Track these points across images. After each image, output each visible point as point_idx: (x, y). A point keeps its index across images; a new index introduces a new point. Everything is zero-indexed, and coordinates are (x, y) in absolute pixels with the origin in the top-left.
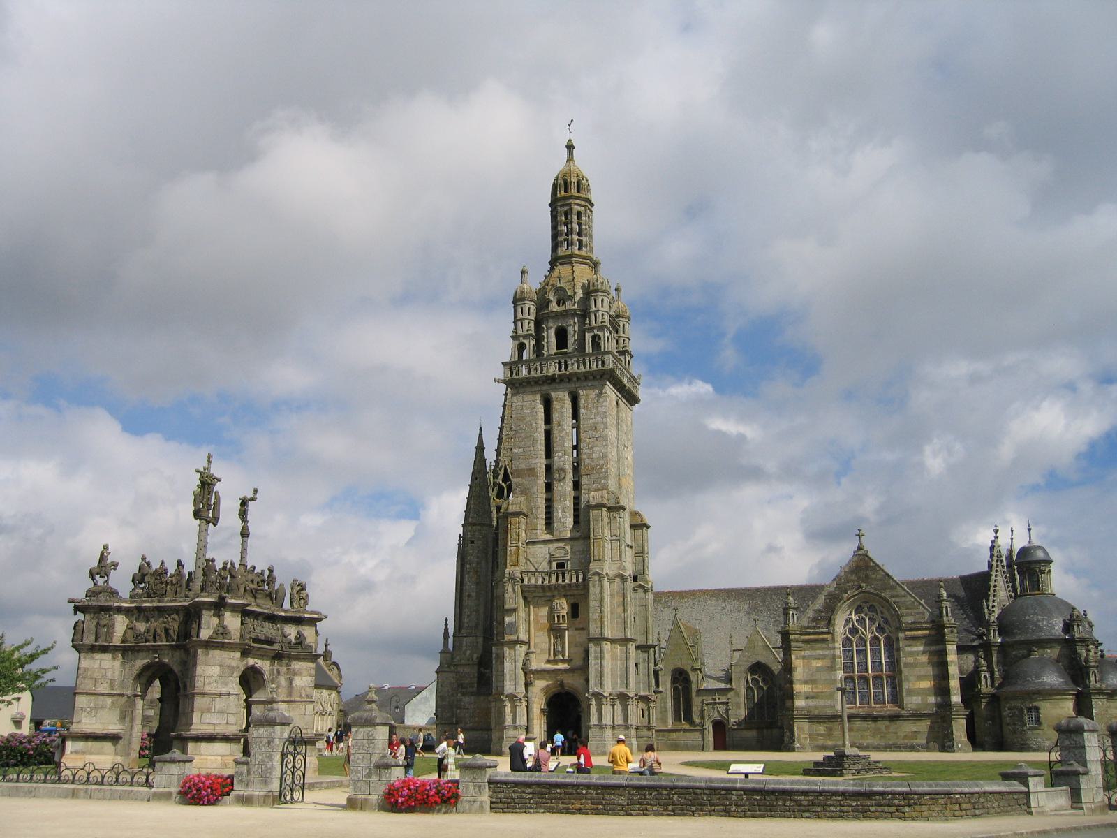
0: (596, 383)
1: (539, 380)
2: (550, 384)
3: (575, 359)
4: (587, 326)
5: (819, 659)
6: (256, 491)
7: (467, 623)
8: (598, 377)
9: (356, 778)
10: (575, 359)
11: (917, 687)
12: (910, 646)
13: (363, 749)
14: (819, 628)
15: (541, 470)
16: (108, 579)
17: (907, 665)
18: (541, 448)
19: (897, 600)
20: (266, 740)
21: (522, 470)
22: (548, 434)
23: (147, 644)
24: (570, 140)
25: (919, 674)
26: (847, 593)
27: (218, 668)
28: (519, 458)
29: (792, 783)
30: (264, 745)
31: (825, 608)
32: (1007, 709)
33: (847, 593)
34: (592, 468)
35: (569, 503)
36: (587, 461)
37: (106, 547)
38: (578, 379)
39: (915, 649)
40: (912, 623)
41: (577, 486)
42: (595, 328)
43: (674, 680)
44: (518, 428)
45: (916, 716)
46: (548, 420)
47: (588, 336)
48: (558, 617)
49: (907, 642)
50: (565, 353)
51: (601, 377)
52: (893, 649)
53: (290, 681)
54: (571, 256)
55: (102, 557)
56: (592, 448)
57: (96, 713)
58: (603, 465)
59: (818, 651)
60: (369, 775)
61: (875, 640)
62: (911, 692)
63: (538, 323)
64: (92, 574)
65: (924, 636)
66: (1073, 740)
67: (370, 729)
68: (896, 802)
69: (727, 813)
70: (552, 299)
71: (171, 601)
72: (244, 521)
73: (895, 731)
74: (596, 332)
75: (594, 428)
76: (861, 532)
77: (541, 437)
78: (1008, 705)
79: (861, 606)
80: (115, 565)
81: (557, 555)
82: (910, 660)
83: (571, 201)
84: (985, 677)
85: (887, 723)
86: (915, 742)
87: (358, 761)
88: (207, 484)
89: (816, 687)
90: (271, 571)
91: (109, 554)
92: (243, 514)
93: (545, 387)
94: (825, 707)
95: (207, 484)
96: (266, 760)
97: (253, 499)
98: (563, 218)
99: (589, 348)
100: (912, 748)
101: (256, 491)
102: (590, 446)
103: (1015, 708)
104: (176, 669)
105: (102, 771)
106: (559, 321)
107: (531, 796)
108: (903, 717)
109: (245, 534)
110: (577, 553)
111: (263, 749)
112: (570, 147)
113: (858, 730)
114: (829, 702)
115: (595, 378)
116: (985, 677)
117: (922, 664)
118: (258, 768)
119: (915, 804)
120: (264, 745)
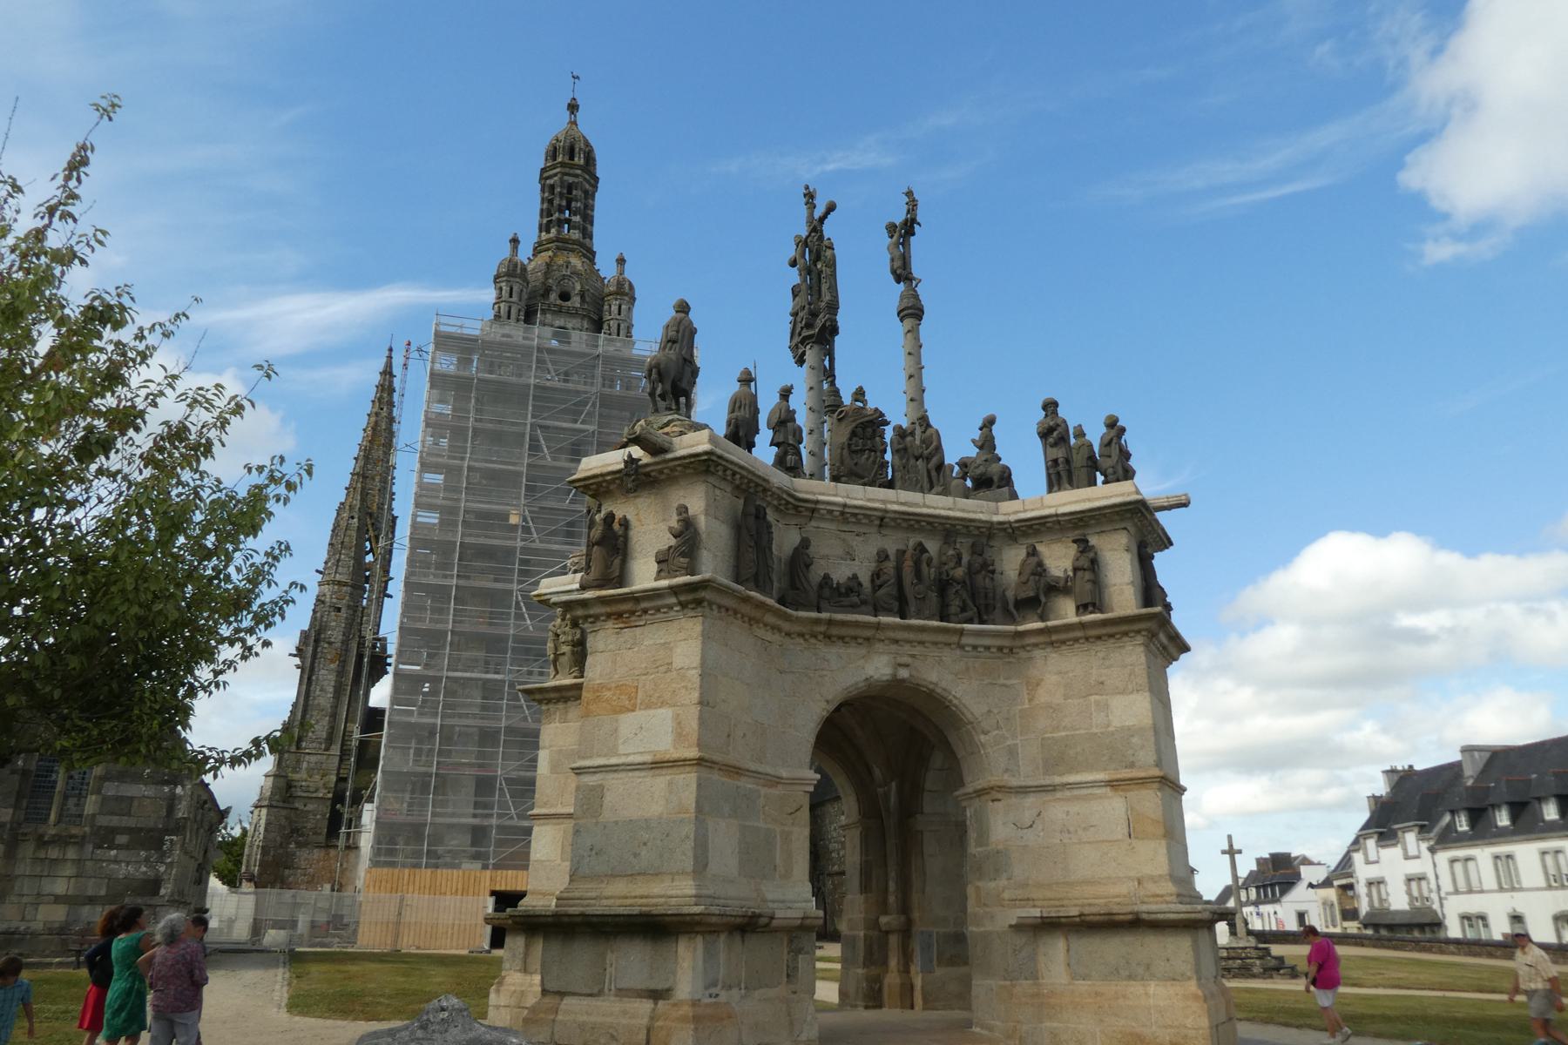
37: (683, 308)
70: (554, 288)
83: (579, 172)
98: (565, 191)
106: (562, 320)
112: (573, 107)
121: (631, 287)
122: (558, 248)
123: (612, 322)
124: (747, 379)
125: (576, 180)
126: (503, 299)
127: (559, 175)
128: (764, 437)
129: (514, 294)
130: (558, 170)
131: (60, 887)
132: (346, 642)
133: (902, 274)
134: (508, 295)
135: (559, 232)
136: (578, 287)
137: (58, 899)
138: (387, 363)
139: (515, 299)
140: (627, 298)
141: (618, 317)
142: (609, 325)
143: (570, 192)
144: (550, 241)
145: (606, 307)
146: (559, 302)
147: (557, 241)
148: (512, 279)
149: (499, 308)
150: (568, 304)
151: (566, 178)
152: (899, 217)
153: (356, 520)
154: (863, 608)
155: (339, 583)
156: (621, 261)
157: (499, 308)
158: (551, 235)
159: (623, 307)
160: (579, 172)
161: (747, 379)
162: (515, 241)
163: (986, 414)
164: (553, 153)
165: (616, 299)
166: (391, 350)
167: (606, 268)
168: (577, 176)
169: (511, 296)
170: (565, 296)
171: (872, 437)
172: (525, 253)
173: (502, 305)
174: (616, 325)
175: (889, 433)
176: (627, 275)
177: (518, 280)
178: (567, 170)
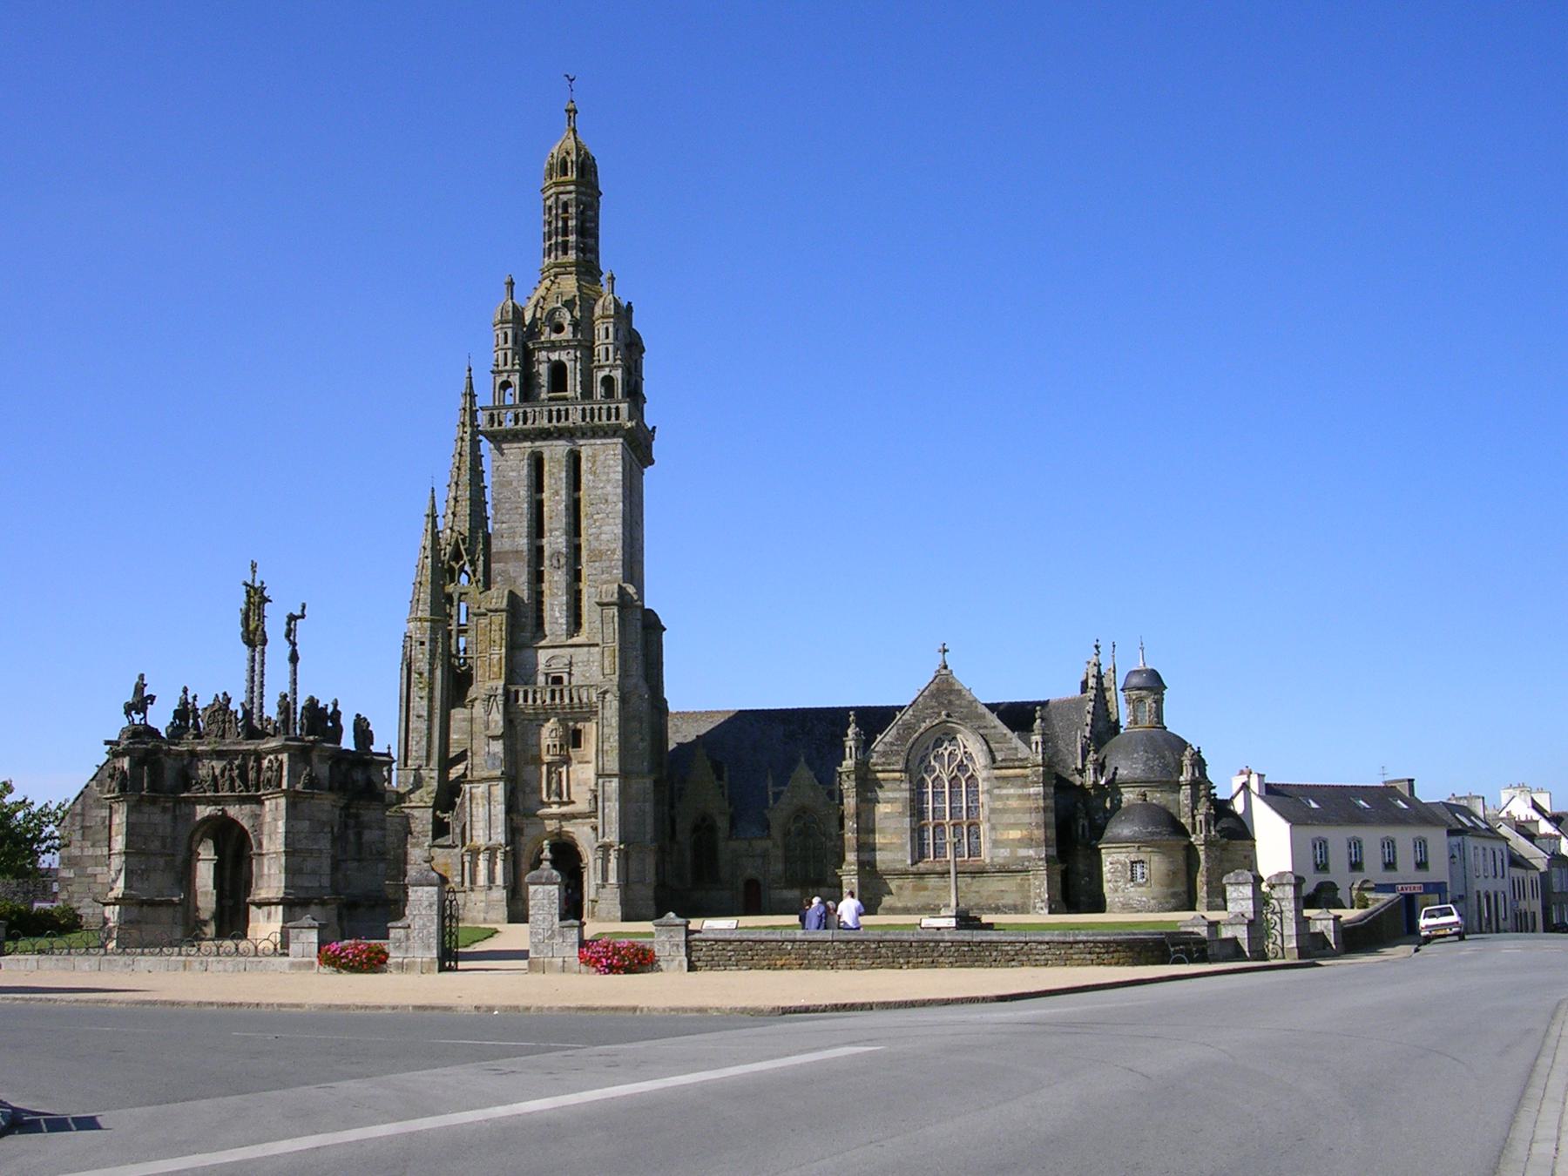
1: (530, 433)
4: (596, 363)
5: (888, 802)
6: (304, 607)
7: (416, 751)
8: (610, 433)
9: (537, 940)
11: (1005, 837)
12: (998, 788)
13: (543, 910)
14: (889, 764)
16: (145, 717)
21: (506, 552)
23: (208, 794)
25: (1008, 821)
26: (925, 722)
27: (308, 822)
28: (502, 537)
29: (987, 935)
31: (897, 740)
32: (1108, 863)
33: (925, 722)
37: (142, 677)
39: (1004, 792)
40: (1003, 760)
42: (608, 366)
43: (696, 829)
44: (501, 496)
45: (1004, 870)
49: (996, 783)
50: (565, 399)
52: (978, 791)
53: (359, 835)
55: (140, 688)
56: (600, 527)
57: (148, 877)
59: (887, 793)
60: (551, 937)
61: (954, 781)
64: (128, 713)
65: (1017, 777)
66: (1241, 892)
68: (1097, 950)
69: (934, 964)
71: (234, 743)
72: (294, 644)
73: (977, 889)
75: (604, 501)
79: (940, 739)
80: (152, 698)
81: (553, 666)
82: (999, 805)
84: (1083, 825)
85: (969, 880)
86: (1001, 902)
87: (539, 923)
88: (256, 599)
89: (885, 837)
90: (335, 704)
91: (145, 685)
92: (290, 633)
94: (894, 861)
95: (256, 599)
97: (303, 616)
99: (599, 391)
101: (304, 607)
104: (246, 824)
105: (254, 941)
107: (732, 953)
108: (987, 872)
109: (294, 658)
110: (580, 664)
111: (424, 912)
113: (934, 888)
114: (899, 856)
116: (1083, 825)
117: (1014, 811)
118: (419, 933)
119: (1114, 952)
120: (425, 908)
123: (601, 347)
124: (185, 691)
126: (499, 347)
130: (552, 191)
134: (503, 342)
139: (510, 344)
146: (554, 337)
151: (561, 196)
153: (430, 560)
154: (202, 790)
161: (185, 691)
165: (603, 323)
169: (506, 342)
173: (499, 352)
174: (604, 350)
178: (561, 189)
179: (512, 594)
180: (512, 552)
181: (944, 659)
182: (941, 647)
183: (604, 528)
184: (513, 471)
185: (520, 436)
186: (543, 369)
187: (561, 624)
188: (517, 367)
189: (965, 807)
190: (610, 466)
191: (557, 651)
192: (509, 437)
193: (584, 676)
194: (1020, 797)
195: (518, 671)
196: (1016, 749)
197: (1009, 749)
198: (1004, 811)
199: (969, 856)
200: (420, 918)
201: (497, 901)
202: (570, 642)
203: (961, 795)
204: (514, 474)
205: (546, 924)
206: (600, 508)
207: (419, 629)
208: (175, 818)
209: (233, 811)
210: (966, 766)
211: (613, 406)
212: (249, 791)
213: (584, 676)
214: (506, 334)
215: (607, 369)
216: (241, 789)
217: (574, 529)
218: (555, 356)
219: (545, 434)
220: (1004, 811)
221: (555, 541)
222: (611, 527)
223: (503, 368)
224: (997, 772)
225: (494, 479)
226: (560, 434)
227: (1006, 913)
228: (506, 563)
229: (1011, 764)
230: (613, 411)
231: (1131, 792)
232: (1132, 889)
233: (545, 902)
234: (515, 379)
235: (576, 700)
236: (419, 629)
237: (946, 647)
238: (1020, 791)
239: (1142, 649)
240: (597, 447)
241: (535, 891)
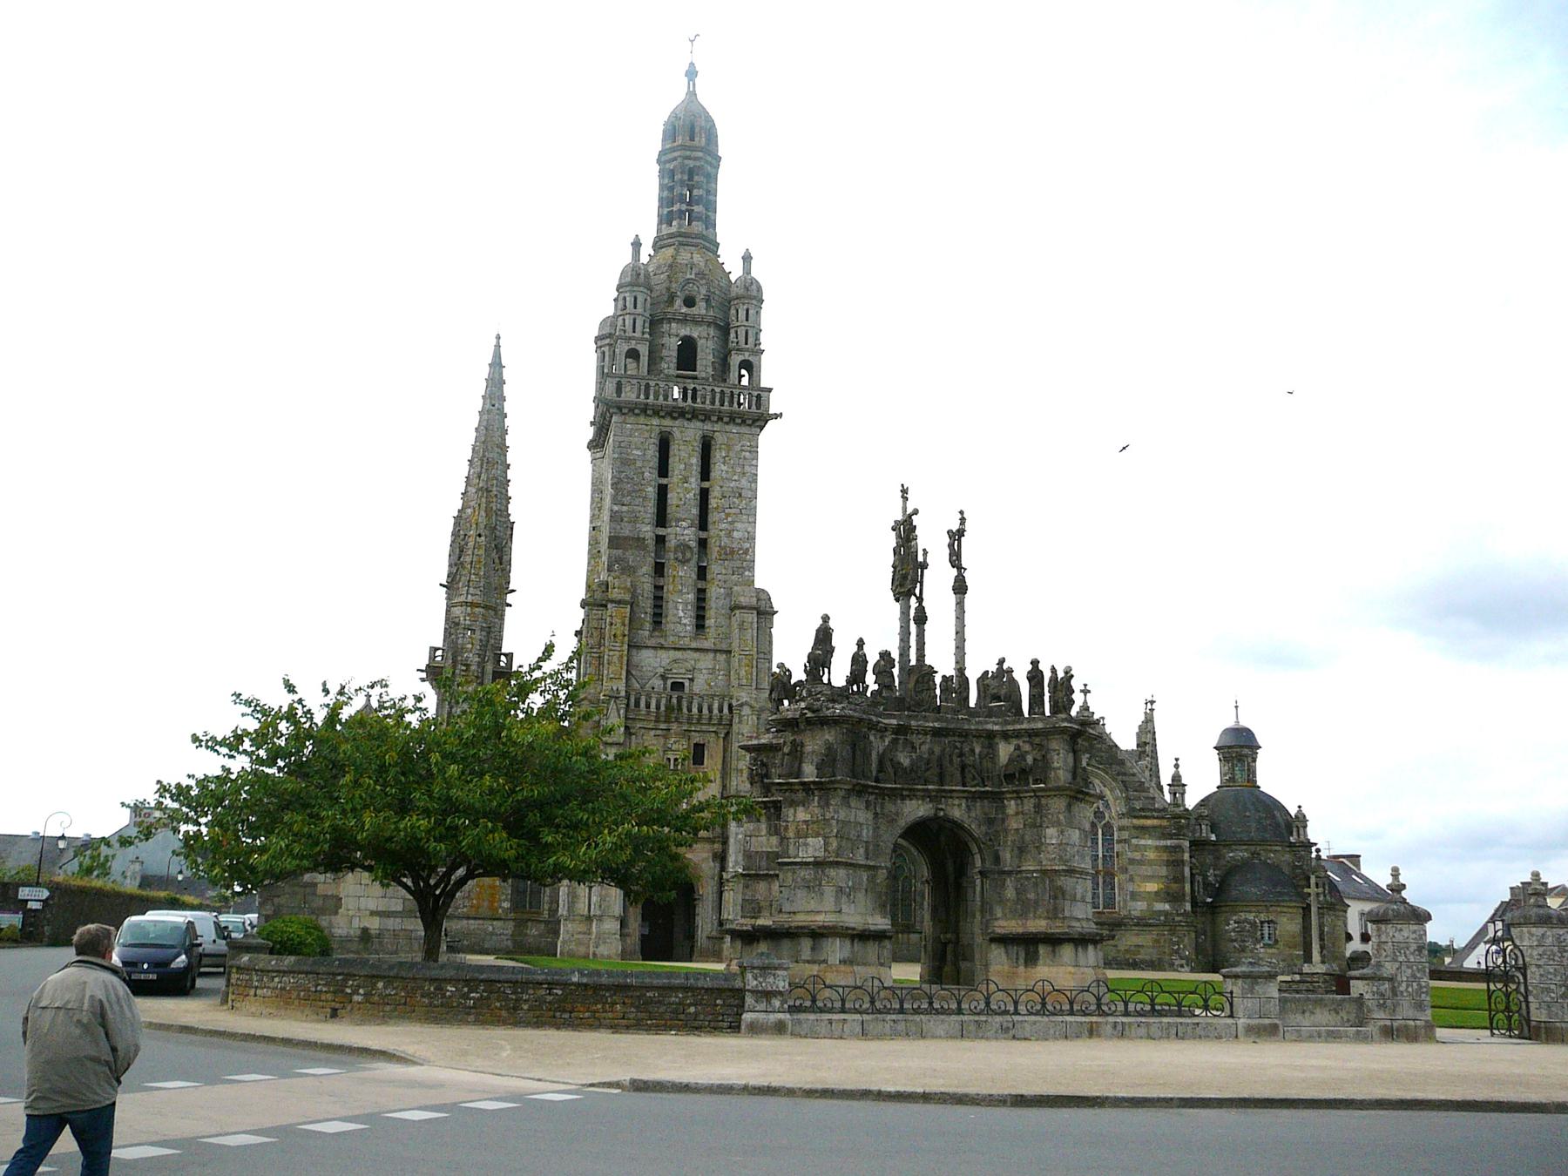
0: (744, 429)
2: (675, 419)
3: (709, 388)
9: (1549, 999)
10: (709, 388)
11: (1142, 890)
13: (1554, 960)
15: (651, 543)
17: (1132, 861)
18: (651, 508)
19: (1125, 778)
20: (1413, 947)
21: (626, 538)
22: (662, 492)
24: (692, 64)
27: (1077, 831)
28: (622, 521)
30: (1412, 954)
32: (1232, 922)
34: (732, 552)
35: (691, 597)
36: (725, 541)
37: (826, 619)
38: (720, 419)
39: (1142, 842)
40: (1142, 810)
41: (702, 573)
42: (747, 350)
45: (1142, 923)
46: (663, 470)
47: (735, 360)
48: (676, 760)
51: (754, 421)
54: (698, 236)
56: (732, 523)
58: (747, 549)
62: (1134, 896)
63: (655, 323)
65: (1154, 827)
67: (1561, 932)
74: (746, 356)
76: (1088, 688)
77: (651, 491)
78: (1234, 918)
81: (675, 671)
82: (1137, 855)
83: (700, 154)
93: (668, 422)
95: (906, 531)
96: (1418, 975)
98: (686, 178)
100: (1135, 965)
102: (730, 519)
103: (1246, 921)
106: (688, 329)
110: (704, 671)
112: (692, 74)
115: (744, 422)
117: (1151, 863)
118: (1407, 987)
121: (759, 289)
122: (681, 244)
124: (861, 643)
125: (698, 164)
127: (679, 160)
128: (870, 678)
129: (639, 306)
131: (372, 905)
132: (481, 665)
133: (955, 559)
135: (680, 226)
136: (703, 291)
137: (373, 913)
138: (495, 352)
139: (640, 310)
140: (754, 302)
141: (745, 323)
142: (736, 332)
143: (691, 179)
144: (671, 236)
145: (733, 311)
146: (684, 310)
147: (680, 236)
148: (635, 289)
149: (624, 320)
150: (694, 310)
151: (686, 162)
152: (955, 527)
155: (472, 605)
156: (747, 259)
157: (624, 320)
158: (673, 229)
159: (750, 312)
160: (700, 154)
161: (861, 643)
162: (637, 245)
163: (1001, 657)
164: (671, 132)
166: (498, 337)
167: (733, 266)
168: (696, 159)
169: (635, 307)
170: (690, 302)
171: (928, 682)
172: (646, 251)
173: (627, 317)
174: (744, 333)
175: (938, 679)
176: (753, 274)
177: (642, 289)
178: (688, 153)
179: (633, 591)
180: (633, 538)
181: (1085, 701)
182: (1083, 688)
183: (736, 524)
184: (638, 449)
185: (648, 412)
186: (673, 344)
187: (685, 625)
188: (647, 336)
189: (1100, 856)
190: (745, 458)
191: (679, 654)
192: (637, 411)
193: (709, 685)
194: (1157, 848)
195: (634, 673)
196: (1154, 798)
197: (1148, 798)
198: (1141, 862)
199: (1104, 908)
200: (1408, 967)
201: (609, 933)
202: (694, 645)
203: (1097, 843)
204: (639, 453)
205: (1559, 978)
206: (734, 503)
207: (469, 615)
208: (876, 814)
209: (957, 811)
210: (1102, 813)
211: (755, 393)
212: (986, 786)
213: (709, 685)
214: (635, 298)
215: (747, 354)
216: (975, 782)
217: (703, 524)
218: (685, 331)
219: (677, 413)
220: (1141, 862)
221: (683, 532)
222: (743, 526)
223: (632, 334)
224: (1136, 822)
225: (616, 456)
226: (694, 415)
227: (1143, 969)
228: (625, 550)
229: (1148, 814)
230: (718, 396)
231: (1246, 850)
232: (1262, 950)
233: (1556, 949)
234: (644, 350)
235: (705, 711)
236: (469, 615)
237: (1088, 688)
238: (1157, 843)
239: (1236, 707)
240: (732, 436)
241: (1543, 935)
